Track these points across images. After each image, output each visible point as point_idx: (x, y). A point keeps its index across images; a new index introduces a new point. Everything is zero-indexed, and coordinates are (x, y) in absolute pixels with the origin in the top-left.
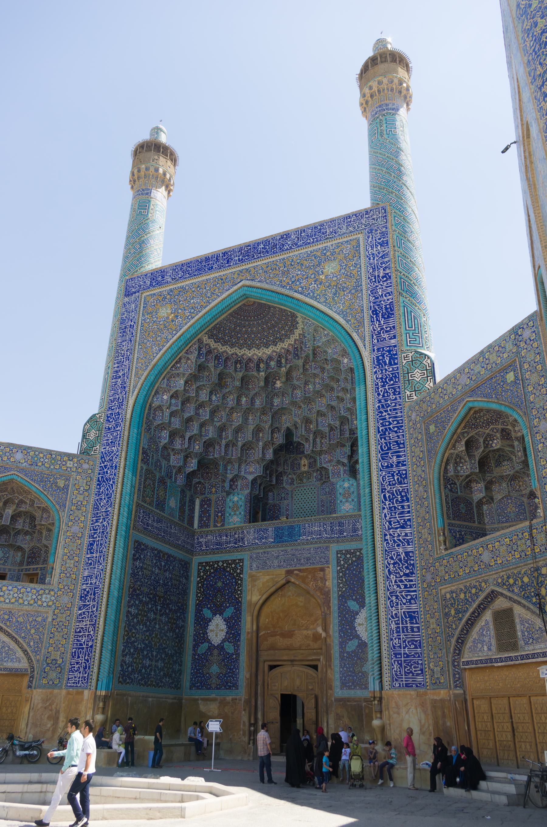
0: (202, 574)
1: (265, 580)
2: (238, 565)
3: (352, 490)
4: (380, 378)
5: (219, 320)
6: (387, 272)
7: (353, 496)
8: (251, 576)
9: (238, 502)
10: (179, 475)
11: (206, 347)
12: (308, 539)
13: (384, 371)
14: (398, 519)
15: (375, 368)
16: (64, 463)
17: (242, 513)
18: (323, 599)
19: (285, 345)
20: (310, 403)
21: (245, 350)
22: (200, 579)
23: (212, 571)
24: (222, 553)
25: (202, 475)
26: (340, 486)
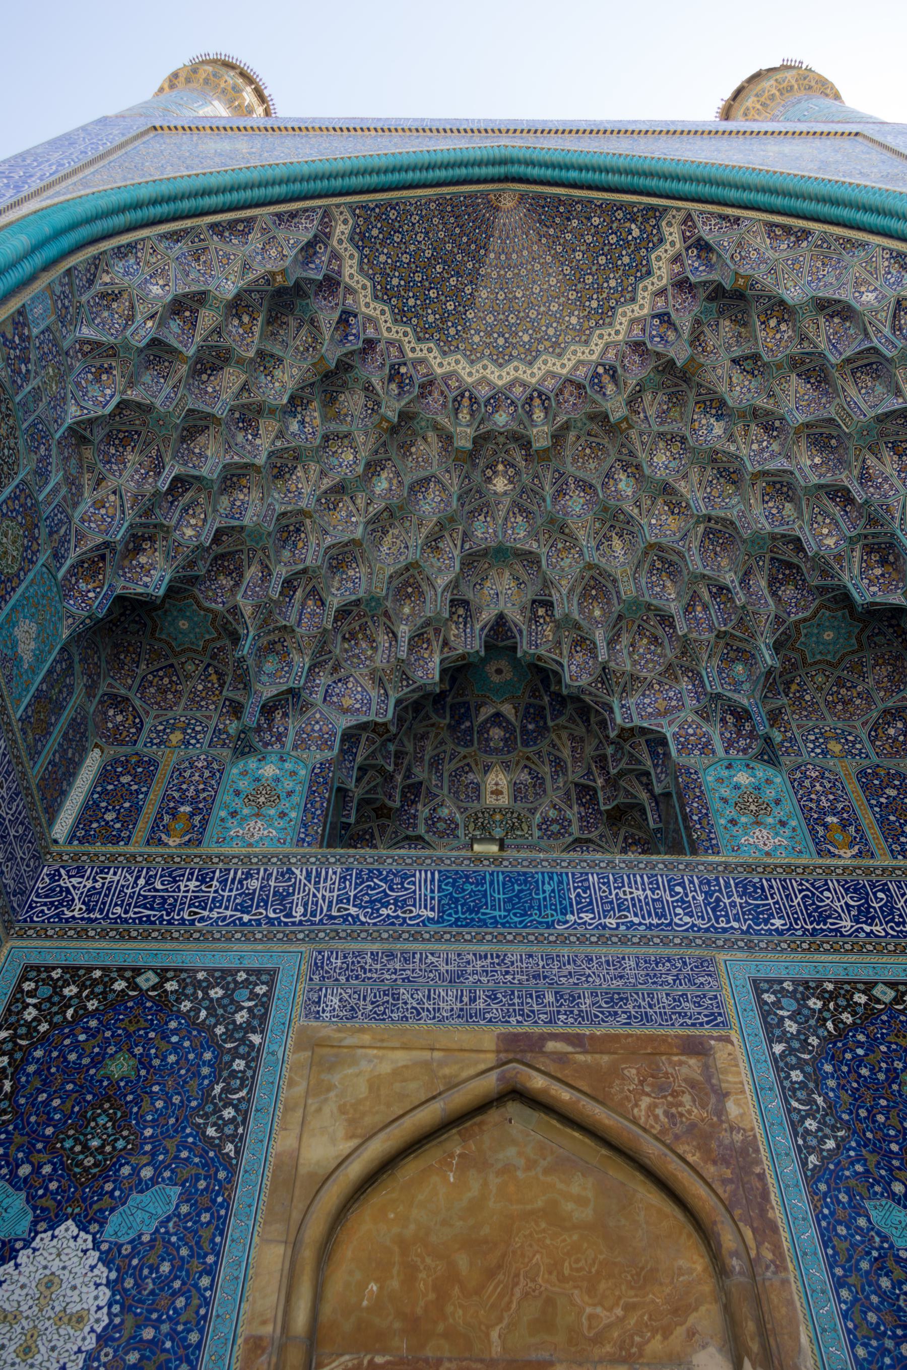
0: (30, 1014)
1: (385, 1068)
2: (242, 995)
3: (770, 794)
5: (405, 193)
7: (779, 813)
8: (311, 1043)
12: (604, 927)
17: (293, 815)
18: (724, 1182)
19: (563, 366)
20: (609, 539)
21: (430, 350)
22: (13, 1038)
23: (92, 1005)
25: (142, 688)
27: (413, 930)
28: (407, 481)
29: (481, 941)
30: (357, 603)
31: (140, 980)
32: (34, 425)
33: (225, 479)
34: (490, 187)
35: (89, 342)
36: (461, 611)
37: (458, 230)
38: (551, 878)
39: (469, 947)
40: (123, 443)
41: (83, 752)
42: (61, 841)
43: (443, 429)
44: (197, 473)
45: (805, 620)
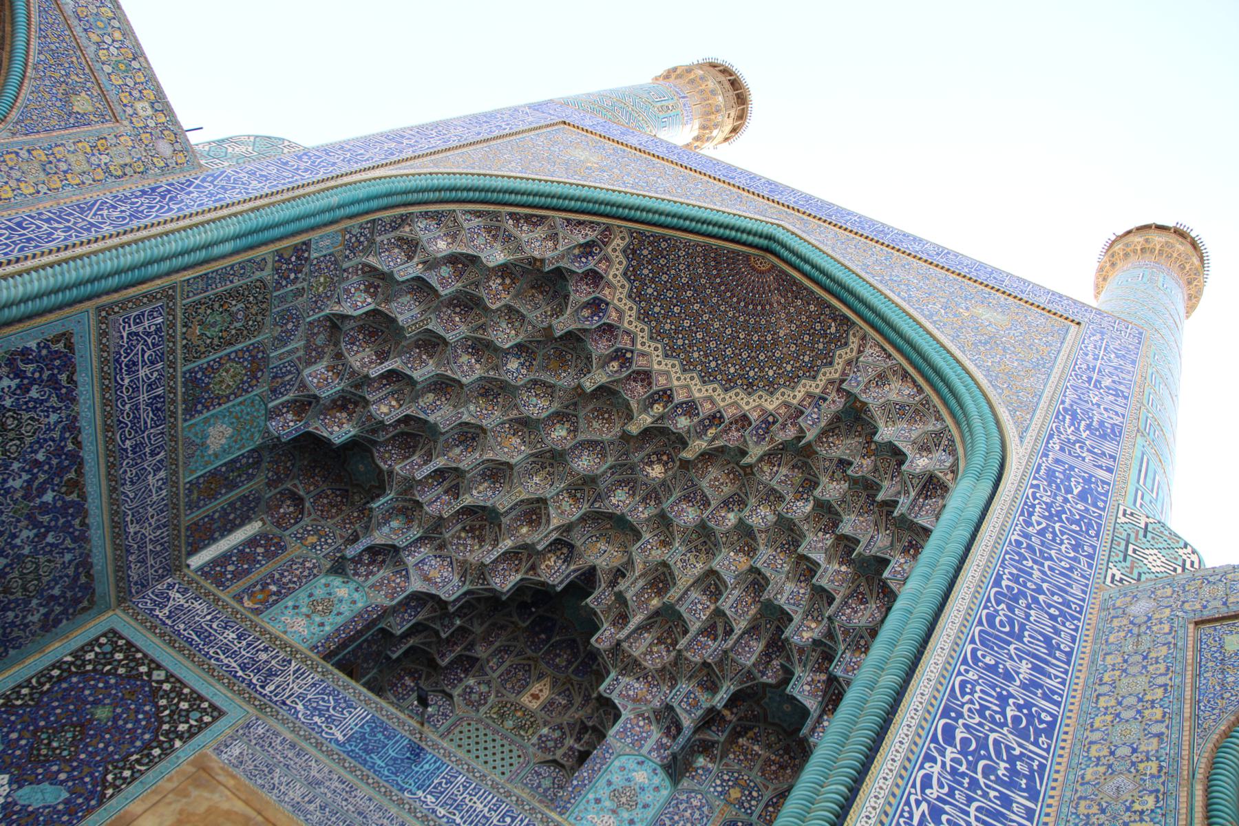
1: (225, 806)
3: (647, 797)
4: (1046, 503)
5: (679, 234)
6: (1122, 388)
7: (638, 814)
9: (341, 601)
10: (290, 416)
11: (600, 261)
12: (434, 811)
13: (1060, 499)
14: (972, 820)
15: (1035, 478)
16: (136, 94)
17: (327, 628)
19: (747, 404)
21: (656, 349)
23: (121, 671)
24: (191, 657)
25: (319, 496)
26: (622, 768)
27: (321, 739)
28: (582, 437)
29: (351, 772)
30: (484, 508)
31: (155, 673)
32: (288, 310)
33: (435, 383)
34: (752, 251)
35: (370, 266)
36: (565, 550)
37: (715, 272)
38: (435, 762)
39: (342, 771)
40: (371, 334)
41: (245, 520)
42: (192, 568)
43: (631, 411)
44: (409, 373)
45: (770, 685)
